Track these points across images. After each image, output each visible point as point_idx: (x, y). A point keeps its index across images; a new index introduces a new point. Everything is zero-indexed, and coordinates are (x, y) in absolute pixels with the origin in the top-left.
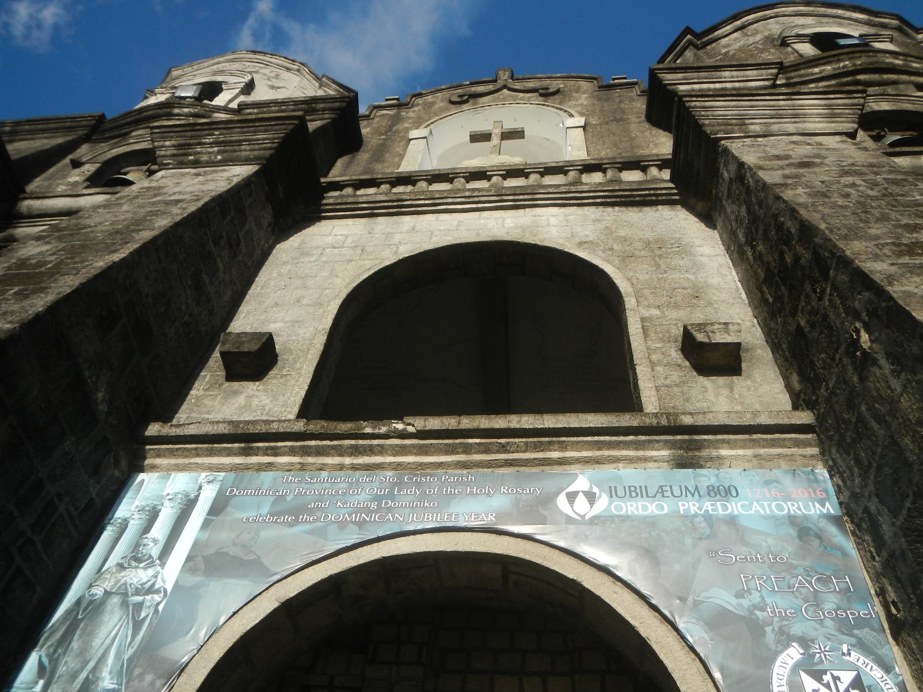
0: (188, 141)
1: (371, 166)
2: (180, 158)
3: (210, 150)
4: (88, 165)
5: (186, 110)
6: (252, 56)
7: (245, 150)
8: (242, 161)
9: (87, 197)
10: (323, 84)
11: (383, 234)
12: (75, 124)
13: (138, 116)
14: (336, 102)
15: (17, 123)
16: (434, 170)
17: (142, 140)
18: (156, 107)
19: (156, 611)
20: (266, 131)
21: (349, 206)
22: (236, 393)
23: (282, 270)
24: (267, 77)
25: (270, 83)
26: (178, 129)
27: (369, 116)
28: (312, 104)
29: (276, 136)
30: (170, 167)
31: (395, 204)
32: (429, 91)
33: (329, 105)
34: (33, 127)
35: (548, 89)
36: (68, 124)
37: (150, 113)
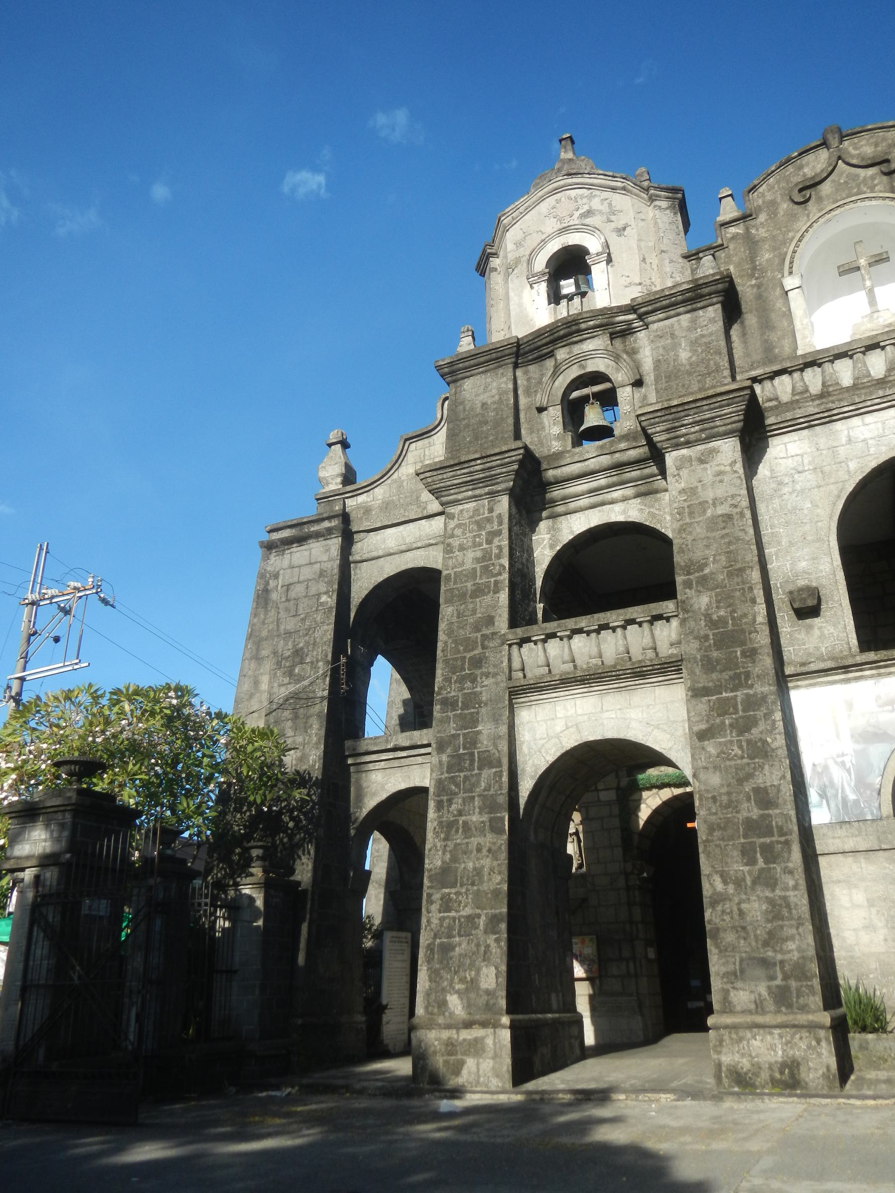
0: (673, 425)
1: (766, 337)
2: (674, 441)
3: (693, 430)
4: (551, 408)
5: (591, 323)
6: (570, 181)
7: (720, 426)
8: (721, 436)
9: (592, 460)
10: (654, 198)
11: (829, 449)
12: (499, 354)
13: (552, 337)
14: (719, 283)
15: (451, 364)
16: (833, 348)
17: (570, 364)
18: (565, 326)
19: (853, 764)
20: (728, 405)
21: (790, 423)
22: (811, 627)
23: (775, 506)
24: (605, 217)
25: (613, 225)
26: (659, 414)
27: (723, 245)
28: (697, 290)
29: (739, 408)
30: (670, 450)
31: (826, 414)
32: (762, 178)
33: (713, 288)
34: (467, 364)
35: (887, 161)
36: (494, 356)
37: (562, 333)
